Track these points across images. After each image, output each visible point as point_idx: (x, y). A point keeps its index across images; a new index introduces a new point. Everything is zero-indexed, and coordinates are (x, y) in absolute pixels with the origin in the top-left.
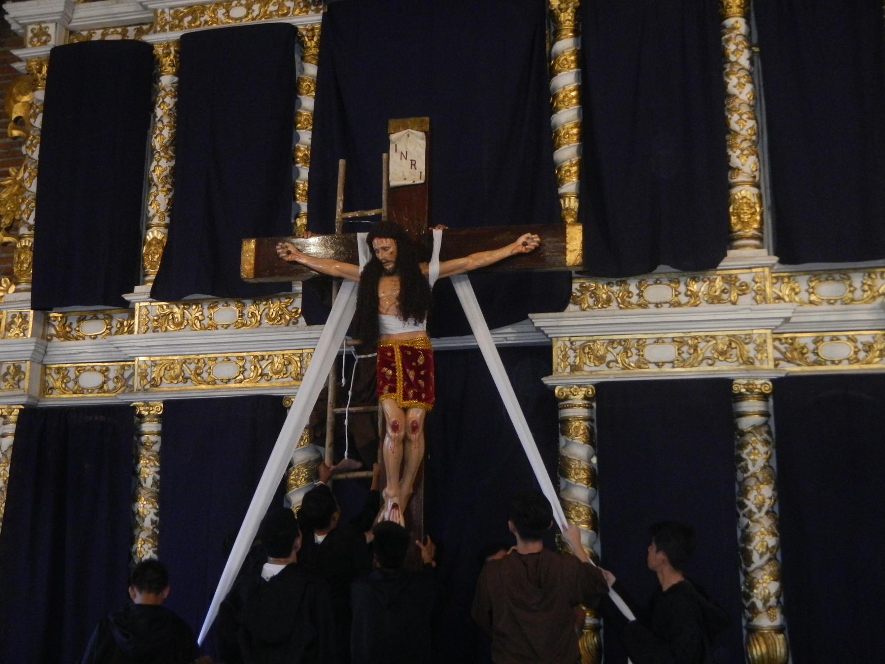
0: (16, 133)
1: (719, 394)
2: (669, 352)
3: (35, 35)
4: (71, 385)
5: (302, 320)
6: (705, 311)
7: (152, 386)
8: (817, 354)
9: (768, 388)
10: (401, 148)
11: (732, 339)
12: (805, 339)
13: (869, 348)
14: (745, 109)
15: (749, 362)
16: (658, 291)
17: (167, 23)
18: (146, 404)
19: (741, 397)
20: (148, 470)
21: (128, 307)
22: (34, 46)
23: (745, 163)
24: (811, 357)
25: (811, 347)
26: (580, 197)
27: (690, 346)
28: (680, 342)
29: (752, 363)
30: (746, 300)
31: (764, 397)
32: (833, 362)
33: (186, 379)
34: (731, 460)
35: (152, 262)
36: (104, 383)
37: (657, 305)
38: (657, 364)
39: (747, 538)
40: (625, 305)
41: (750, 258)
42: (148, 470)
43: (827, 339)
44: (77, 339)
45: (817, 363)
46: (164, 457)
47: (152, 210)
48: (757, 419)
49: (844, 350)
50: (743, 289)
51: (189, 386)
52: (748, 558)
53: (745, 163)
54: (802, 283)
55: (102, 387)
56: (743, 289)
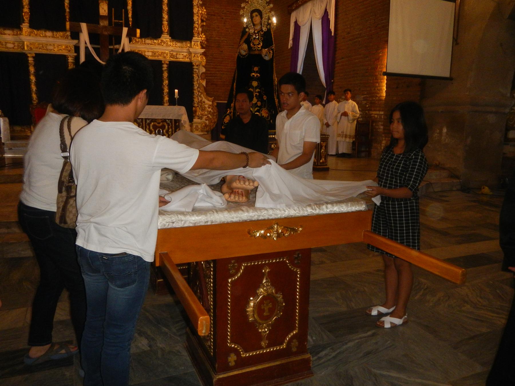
1: (159, 63)
2: (150, 54)
4: (4, 46)
5: (69, 38)
6: (157, 47)
9: (168, 63)
10: (102, 6)
11: (162, 53)
13: (185, 56)
14: (166, 5)
15: (165, 57)
16: (148, 41)
18: (30, 53)
19: (163, 64)
20: (32, 69)
21: (21, 29)
23: (165, 16)
26: (132, 18)
28: (153, 52)
30: (165, 45)
31: (167, 64)
33: (40, 48)
34: (162, 77)
35: (26, 18)
37: (148, 44)
39: (163, 90)
40: (142, 44)
41: (166, 37)
42: (32, 69)
45: (177, 58)
46: (35, 66)
47: (24, 4)
48: (166, 68)
49: (181, 56)
50: (164, 43)
51: (41, 50)
52: (163, 93)
53: (165, 16)
54: (174, 43)
55: (13, 48)
56: (164, 43)
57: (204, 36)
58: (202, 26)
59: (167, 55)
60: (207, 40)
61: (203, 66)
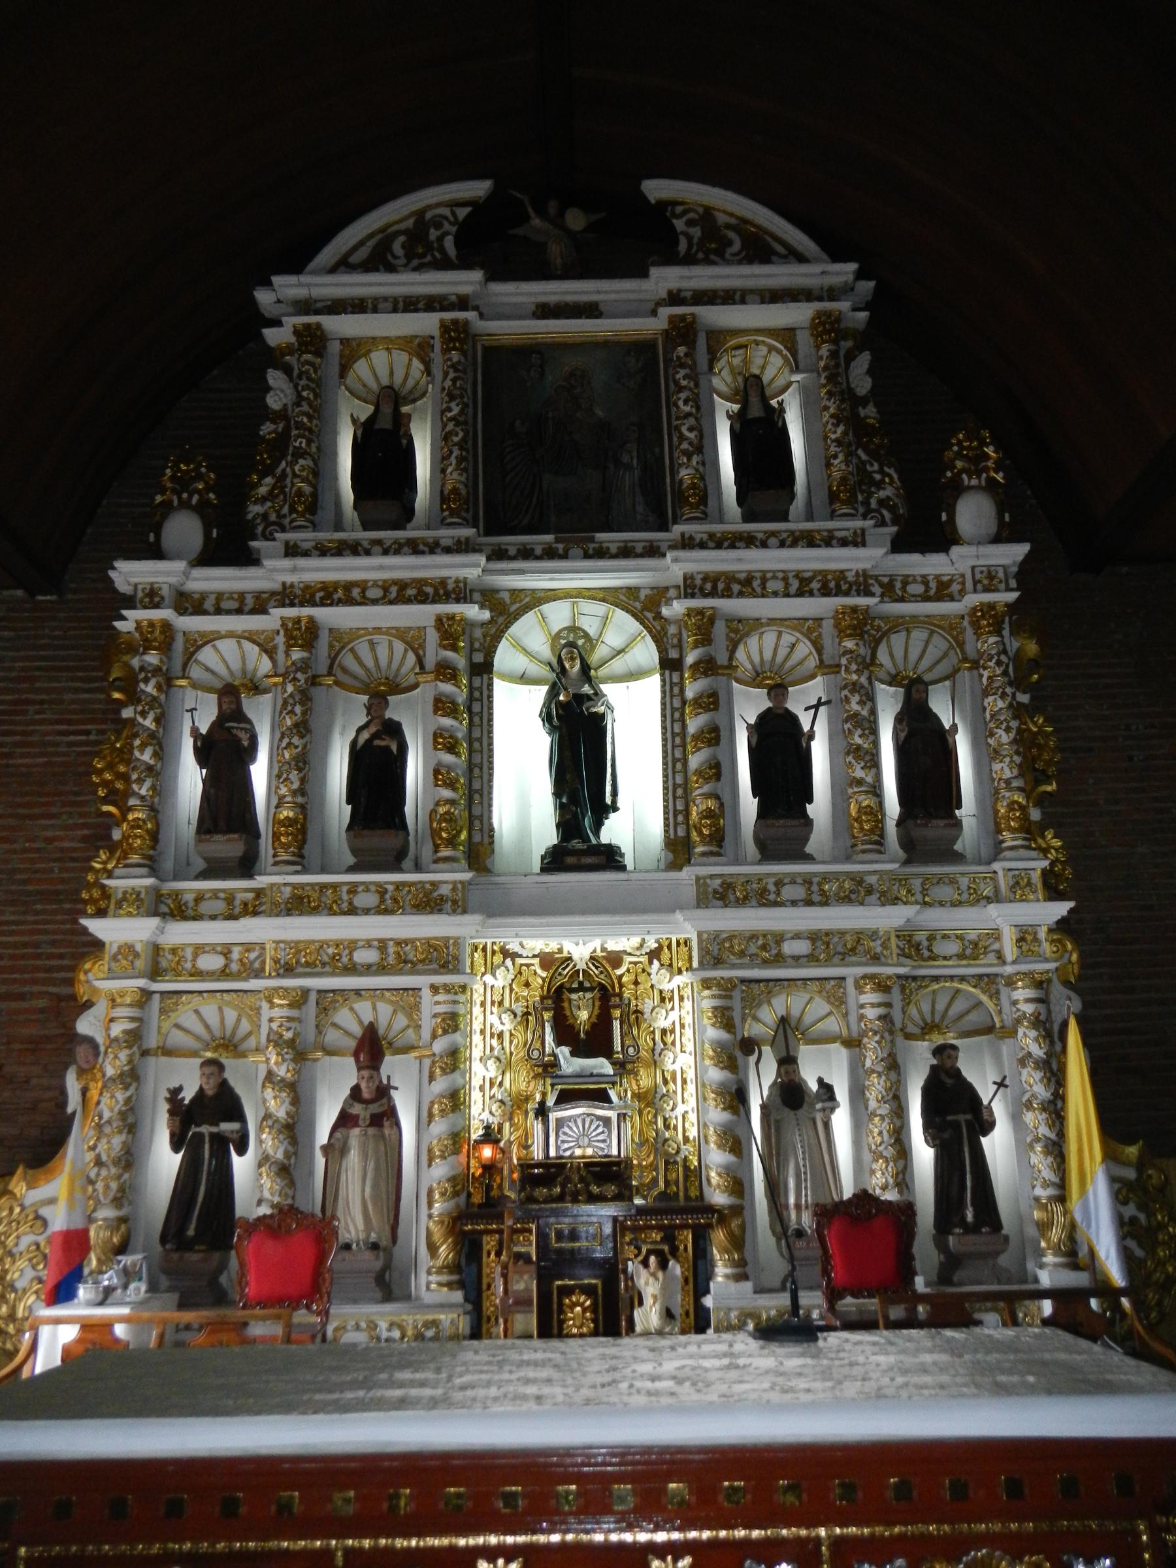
0: (116, 695)
3: (147, 595)
7: (287, 970)
8: (931, 951)
12: (921, 937)
17: (295, 597)
22: (145, 608)
24: (926, 953)
25: (925, 943)
27: (824, 943)
29: (878, 959)
32: (945, 958)
36: (226, 966)
38: (793, 957)
43: (938, 937)
44: (194, 919)
55: (223, 971)
56: (870, 891)
57: (1057, 843)
58: (1042, 801)
59: (885, 946)
60: (1070, 860)
61: (1066, 984)
